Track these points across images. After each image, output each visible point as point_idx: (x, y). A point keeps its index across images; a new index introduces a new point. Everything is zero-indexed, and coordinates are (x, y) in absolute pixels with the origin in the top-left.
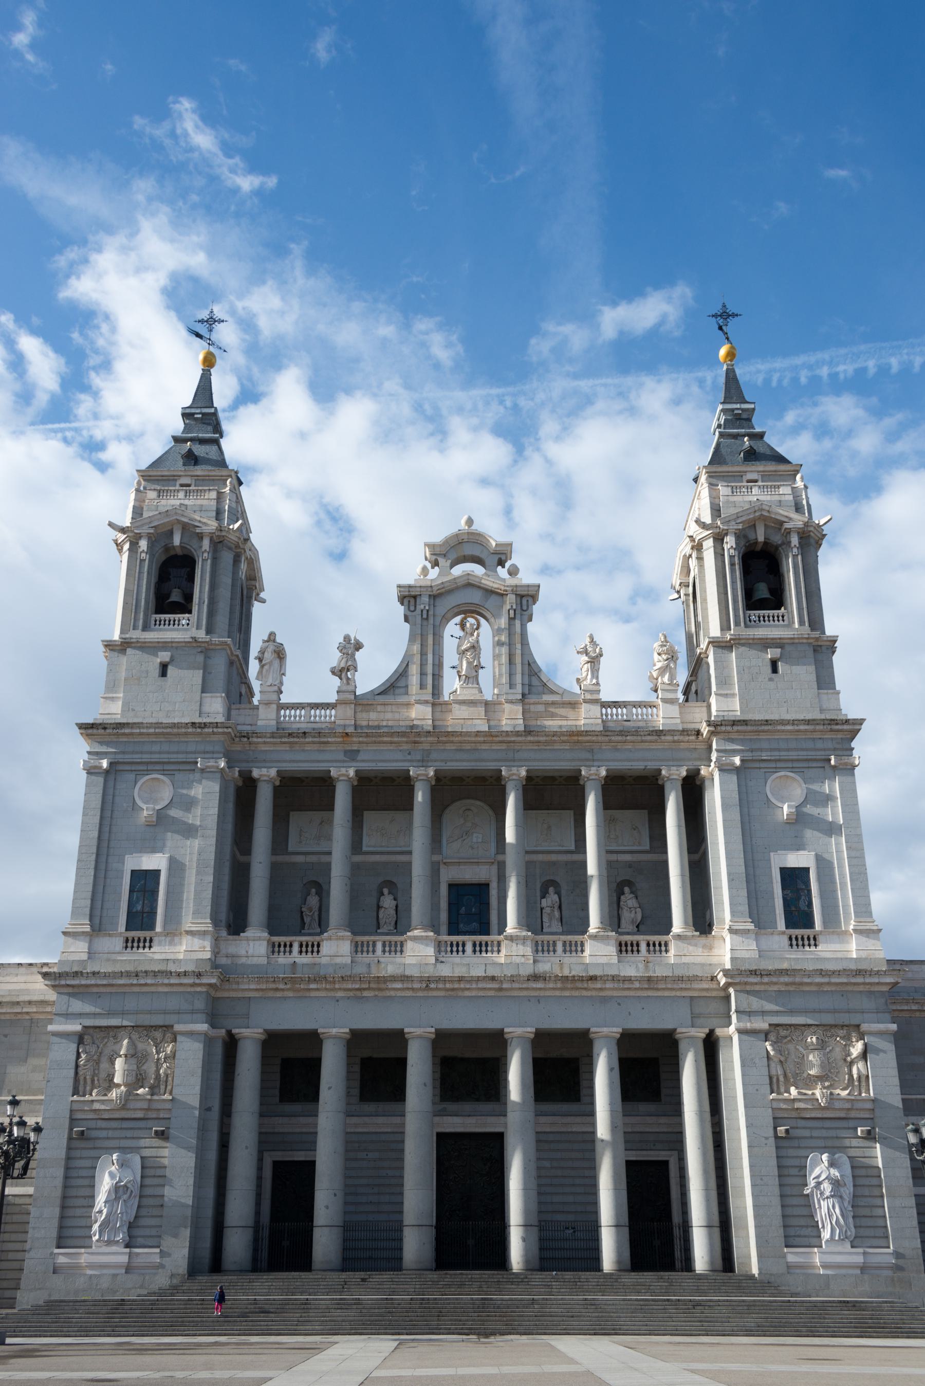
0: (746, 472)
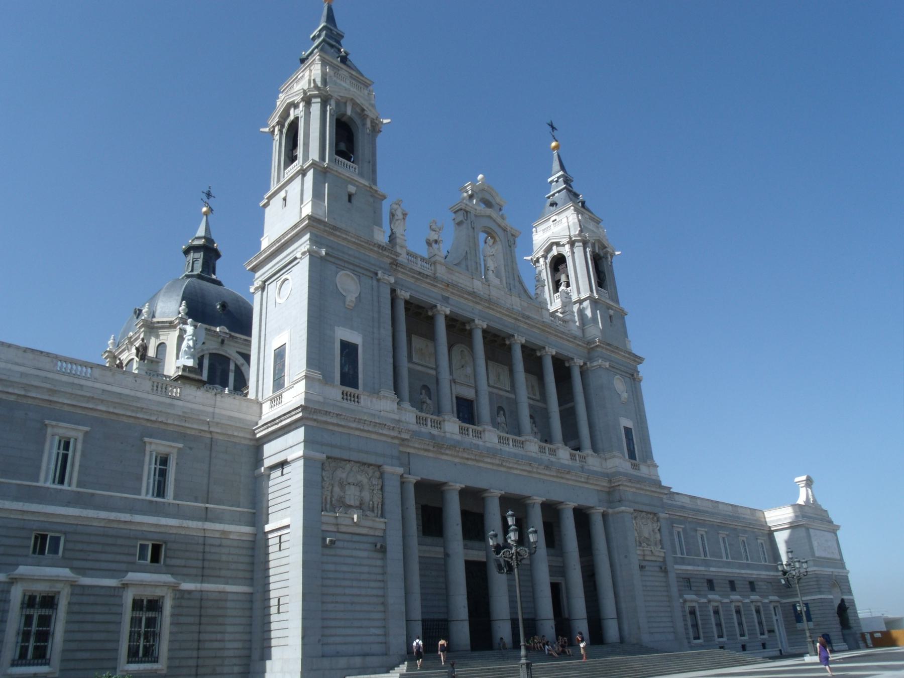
0: (585, 213)
